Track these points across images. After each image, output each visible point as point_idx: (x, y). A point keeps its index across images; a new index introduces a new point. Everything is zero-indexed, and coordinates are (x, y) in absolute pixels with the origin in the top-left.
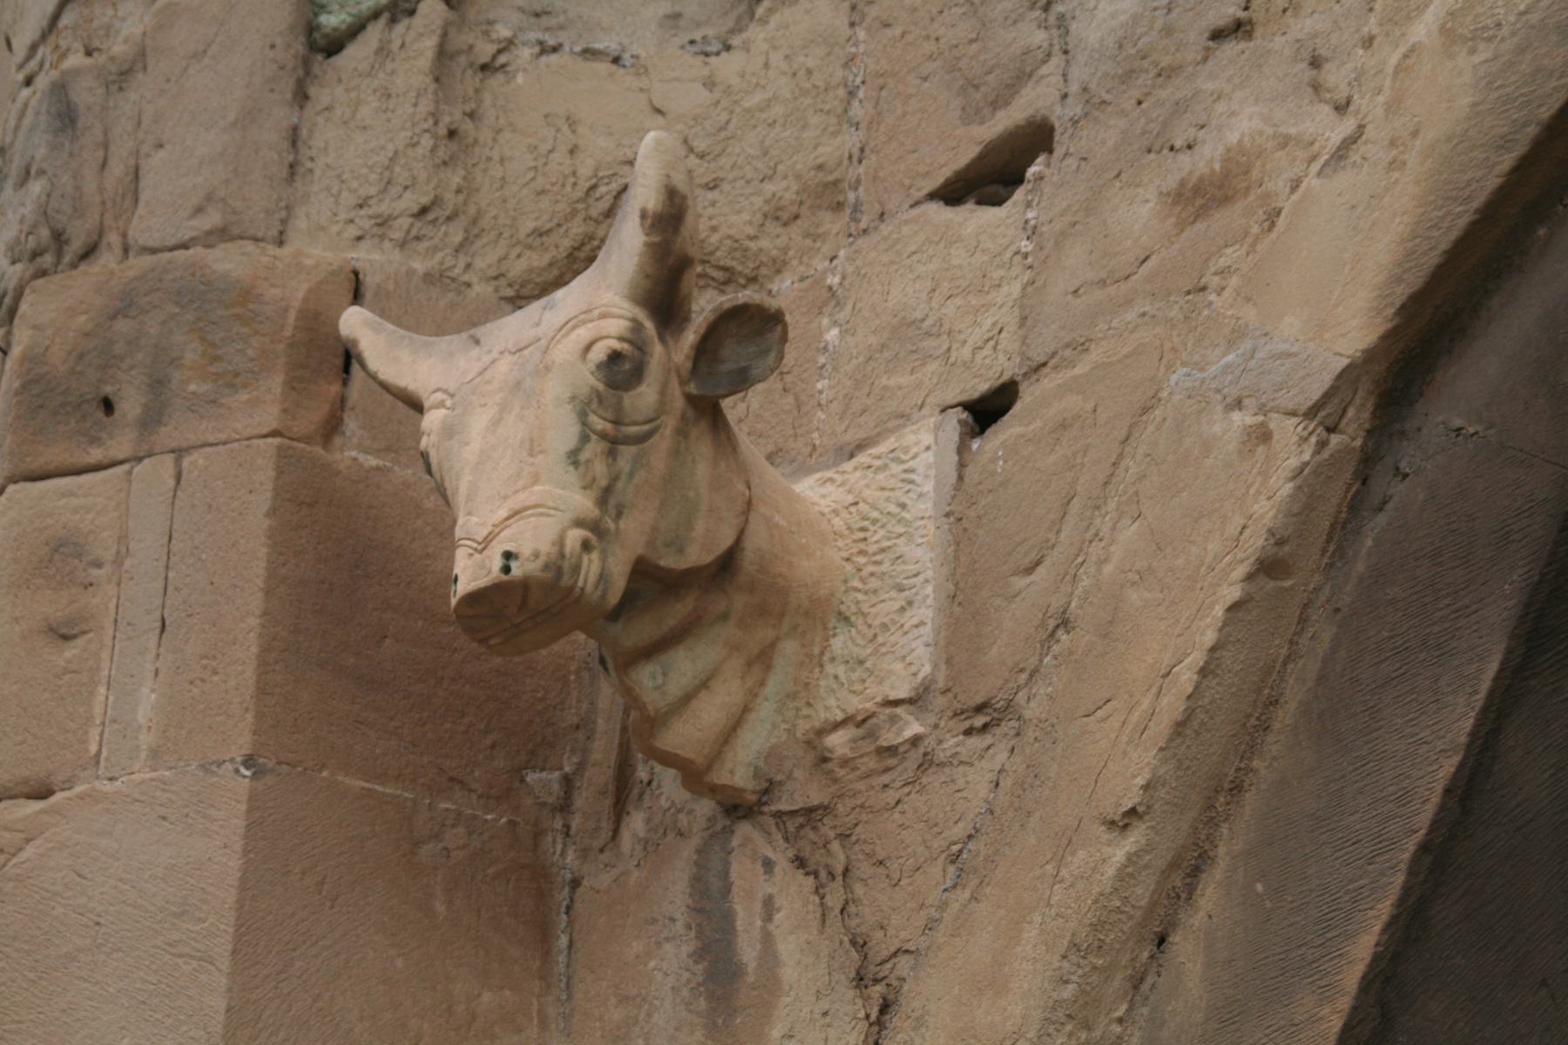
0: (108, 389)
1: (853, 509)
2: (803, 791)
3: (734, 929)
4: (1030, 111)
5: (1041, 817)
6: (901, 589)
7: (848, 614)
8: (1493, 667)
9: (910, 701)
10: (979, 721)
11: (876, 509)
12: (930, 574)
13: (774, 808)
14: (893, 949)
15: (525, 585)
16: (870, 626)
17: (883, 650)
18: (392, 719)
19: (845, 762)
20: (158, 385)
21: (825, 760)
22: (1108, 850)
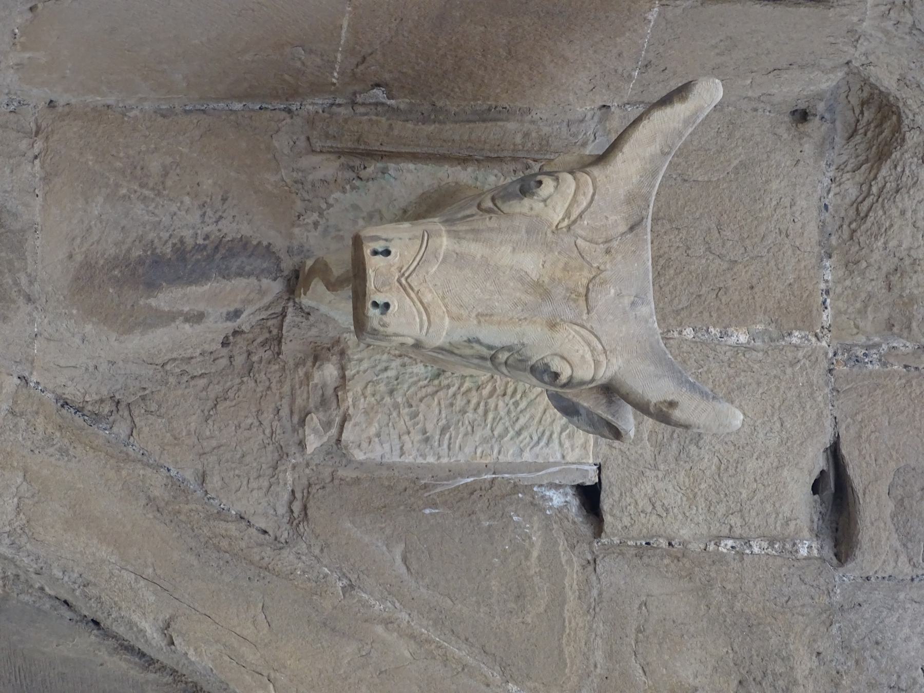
3: (190, 283)
5: (193, 566)
6: (444, 430)
7: (442, 378)
9: (339, 441)
10: (297, 507)
11: (528, 405)
12: (445, 460)
13: (290, 310)
14: (137, 420)
16: (421, 401)
17: (395, 414)
18: (410, 32)
19: (308, 376)
21: (316, 359)
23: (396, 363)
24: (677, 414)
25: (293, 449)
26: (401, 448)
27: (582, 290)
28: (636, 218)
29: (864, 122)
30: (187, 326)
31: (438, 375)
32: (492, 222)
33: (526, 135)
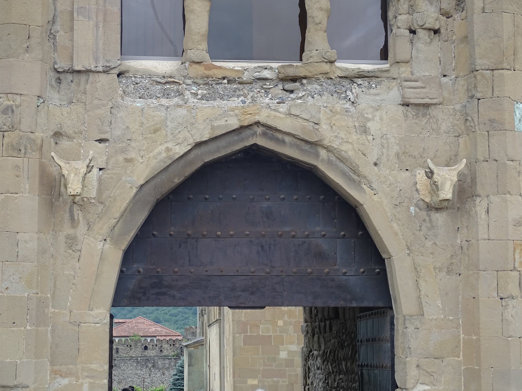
0: (20, 148)
8: (146, 214)
10: (101, 203)
19: (86, 202)
20: (26, 149)
23: (84, 191)
24: (91, 159)
25: (94, 204)
32: (67, 180)
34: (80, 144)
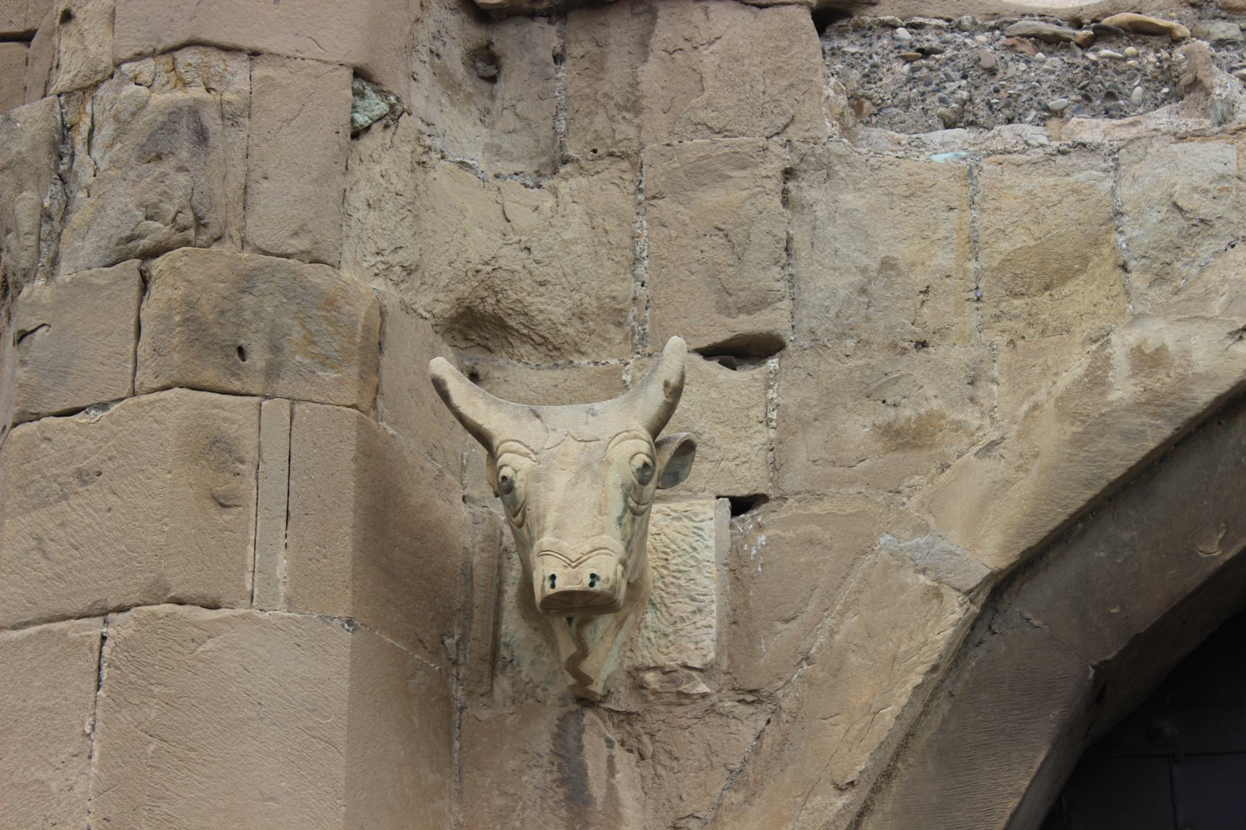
0: (242, 342)
1: (656, 537)
2: (624, 701)
3: (586, 774)
4: (771, 328)
6: (693, 600)
7: (655, 602)
8: (1041, 757)
9: (701, 670)
10: (749, 698)
12: (714, 598)
14: (688, 814)
15: (596, 595)
16: (671, 615)
17: (681, 633)
19: (655, 693)
20: (276, 349)
21: (642, 687)
22: (834, 799)
23: (644, 632)
24: (674, 381)
25: (708, 702)
26: (706, 627)
27: (583, 444)
28: (531, 414)
29: (479, 340)
30: (617, 776)
31: (653, 604)
32: (532, 507)
33: (483, 550)
34: (615, 373)
